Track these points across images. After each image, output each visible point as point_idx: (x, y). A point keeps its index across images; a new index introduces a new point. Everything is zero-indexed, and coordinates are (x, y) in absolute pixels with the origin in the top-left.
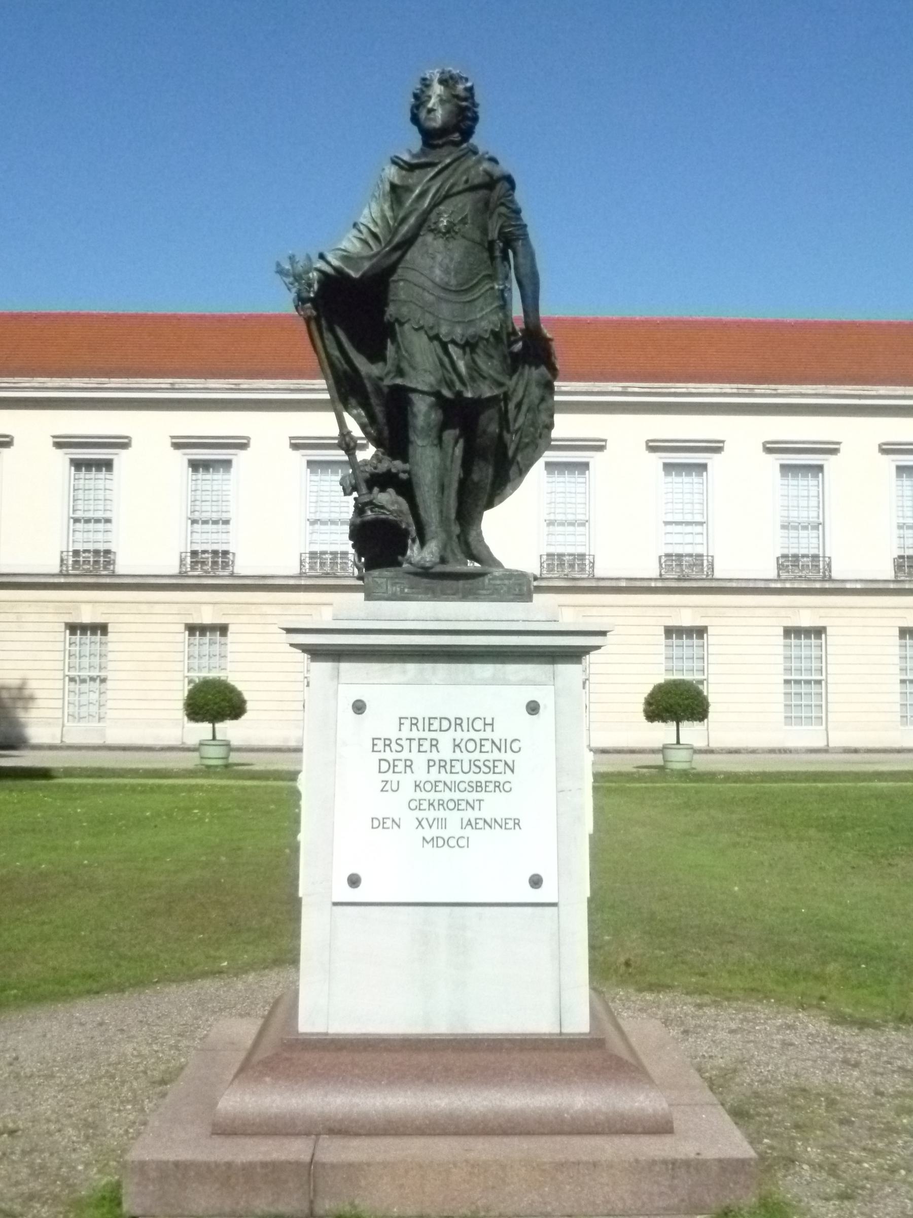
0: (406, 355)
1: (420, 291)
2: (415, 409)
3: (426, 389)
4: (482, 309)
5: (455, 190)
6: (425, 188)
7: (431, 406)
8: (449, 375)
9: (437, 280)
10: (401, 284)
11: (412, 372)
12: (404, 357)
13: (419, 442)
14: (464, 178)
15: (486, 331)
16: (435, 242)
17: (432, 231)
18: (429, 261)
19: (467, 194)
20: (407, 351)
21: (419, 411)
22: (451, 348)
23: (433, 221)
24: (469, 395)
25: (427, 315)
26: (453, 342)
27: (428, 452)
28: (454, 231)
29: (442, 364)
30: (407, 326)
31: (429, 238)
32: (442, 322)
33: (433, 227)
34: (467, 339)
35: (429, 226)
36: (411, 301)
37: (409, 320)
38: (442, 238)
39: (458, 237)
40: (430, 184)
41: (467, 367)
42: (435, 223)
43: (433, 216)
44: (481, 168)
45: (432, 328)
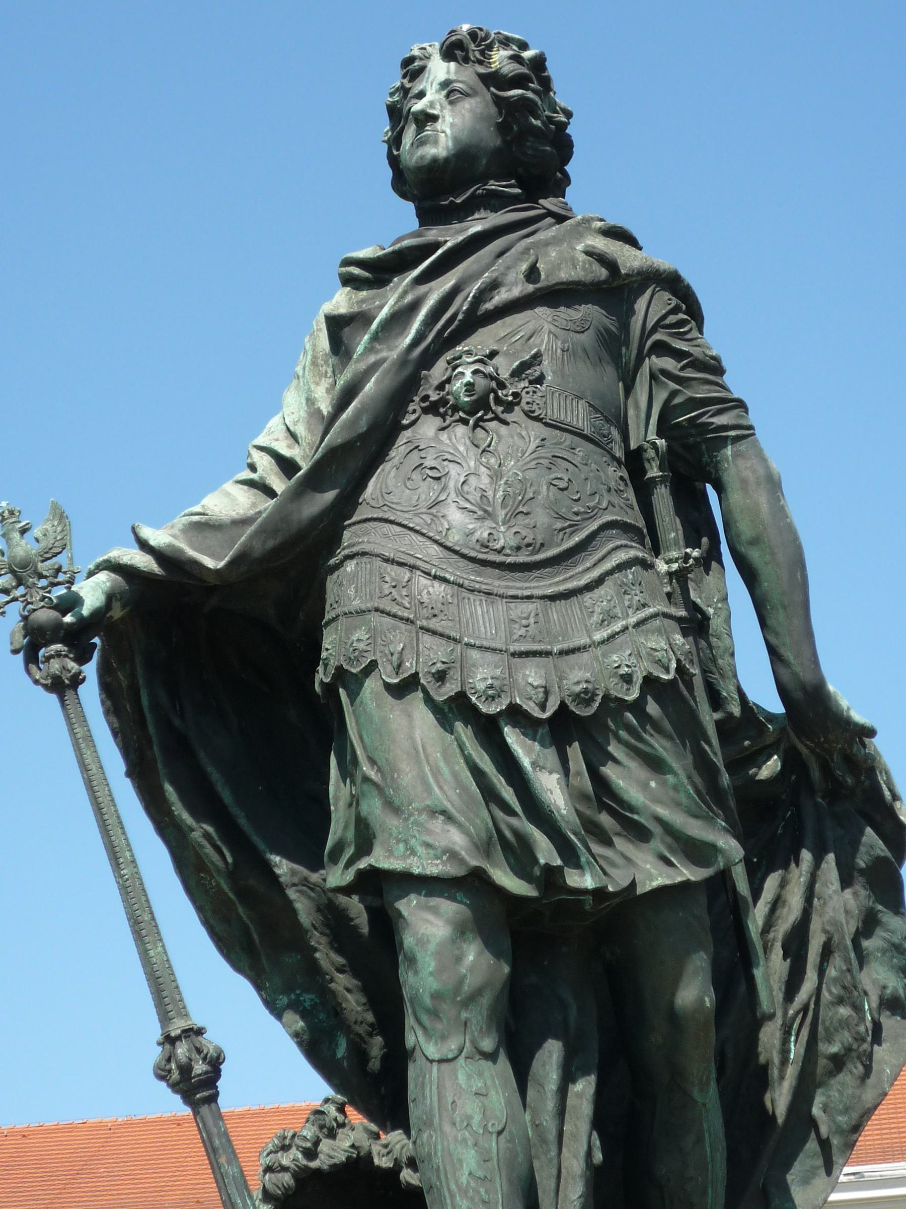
0: (372, 774)
1: (406, 574)
2: (409, 941)
3: (434, 868)
4: (609, 618)
5: (501, 297)
6: (409, 298)
7: (461, 931)
8: (513, 821)
9: (454, 539)
10: (350, 566)
11: (393, 822)
12: (366, 779)
13: (432, 1050)
14: (524, 267)
15: (627, 679)
16: (444, 436)
17: (433, 409)
18: (427, 491)
19: (542, 312)
20: (372, 762)
21: (423, 942)
22: (512, 737)
23: (435, 382)
24: (588, 882)
25: (427, 639)
26: (515, 714)
27: (462, 1078)
28: (498, 401)
29: (490, 795)
30: (371, 685)
31: (429, 426)
32: (475, 654)
33: (434, 397)
34: (563, 705)
35: (426, 398)
36: (377, 610)
37: (373, 665)
38: (465, 422)
39: (517, 415)
40: (423, 289)
41: (576, 796)
42: (441, 387)
43: (438, 371)
44: (580, 247)
45: (441, 677)
